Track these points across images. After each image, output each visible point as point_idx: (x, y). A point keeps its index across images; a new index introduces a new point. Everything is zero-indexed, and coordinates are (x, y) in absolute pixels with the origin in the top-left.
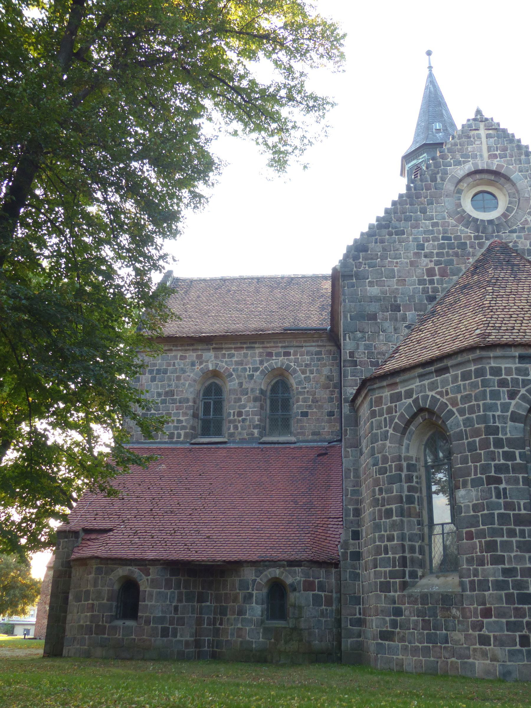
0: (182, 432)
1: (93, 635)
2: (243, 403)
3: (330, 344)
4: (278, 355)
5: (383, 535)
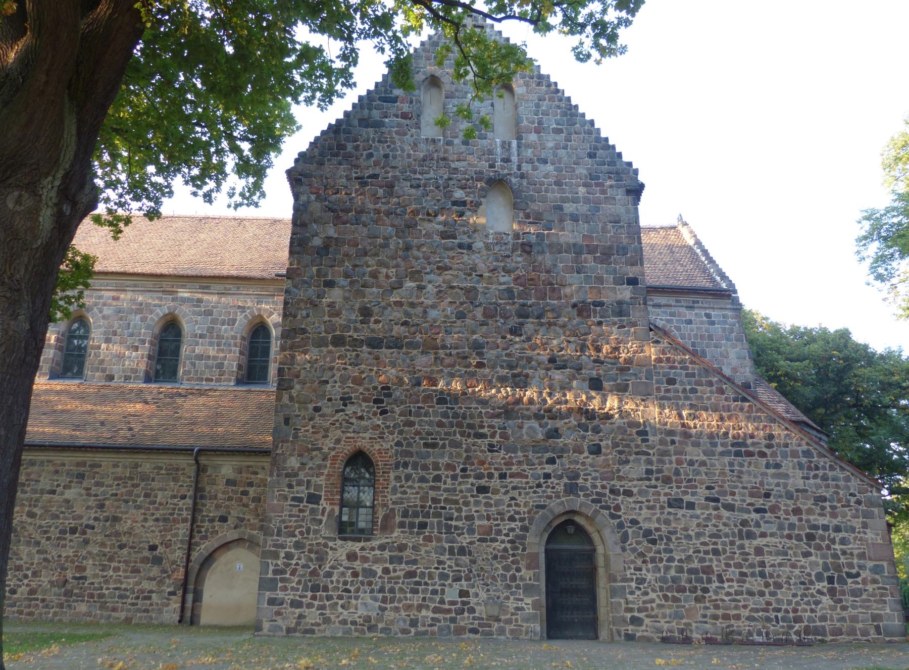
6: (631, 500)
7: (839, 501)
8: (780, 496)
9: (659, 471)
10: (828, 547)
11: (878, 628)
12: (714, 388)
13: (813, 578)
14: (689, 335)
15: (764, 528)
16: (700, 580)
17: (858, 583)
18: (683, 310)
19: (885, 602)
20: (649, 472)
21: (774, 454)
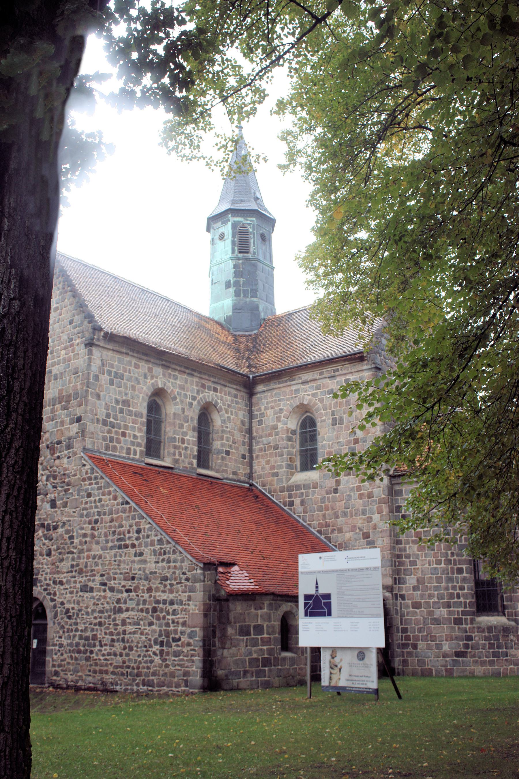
0: (138, 449)
1: (273, 667)
2: (185, 430)
3: (245, 390)
4: (209, 388)
5: (456, 586)
6: (62, 587)
7: (175, 579)
8: (141, 579)
9: (78, 565)
10: (164, 618)
11: (186, 681)
12: (111, 496)
13: (152, 642)
14: (330, 404)
15: (131, 604)
16: (89, 645)
17: (178, 646)
18: (327, 381)
19: (193, 662)
20: (72, 566)
21: (140, 545)
